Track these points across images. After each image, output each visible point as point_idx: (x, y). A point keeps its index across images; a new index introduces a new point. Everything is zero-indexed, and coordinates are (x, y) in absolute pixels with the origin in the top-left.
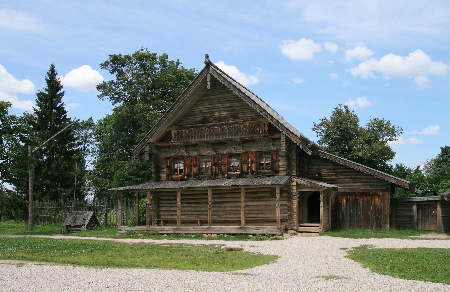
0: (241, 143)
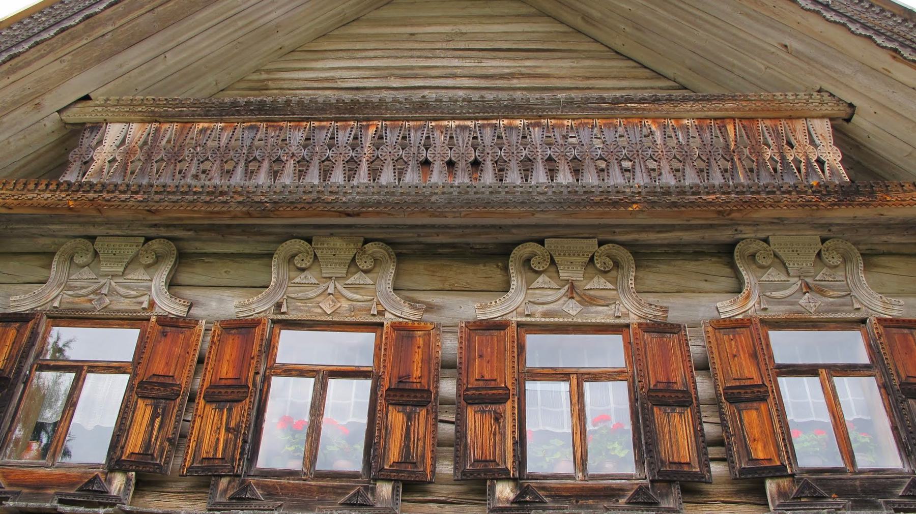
0: (625, 255)
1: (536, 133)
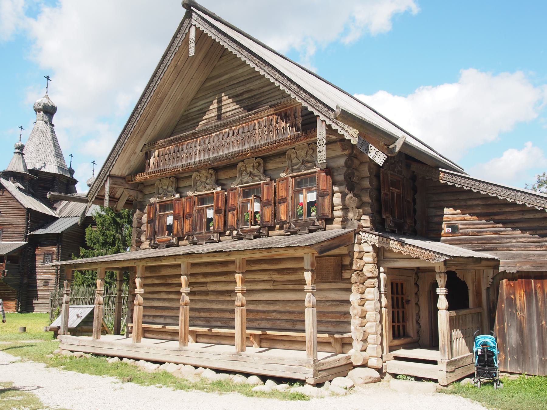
0: (261, 161)
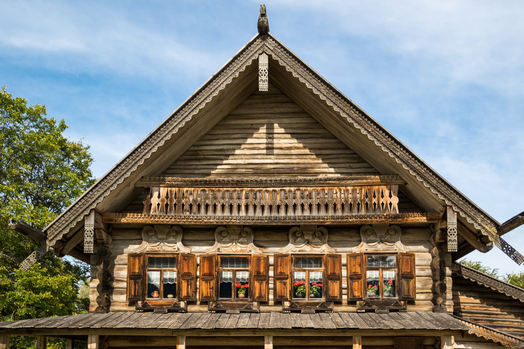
0: (325, 231)
1: (298, 193)
